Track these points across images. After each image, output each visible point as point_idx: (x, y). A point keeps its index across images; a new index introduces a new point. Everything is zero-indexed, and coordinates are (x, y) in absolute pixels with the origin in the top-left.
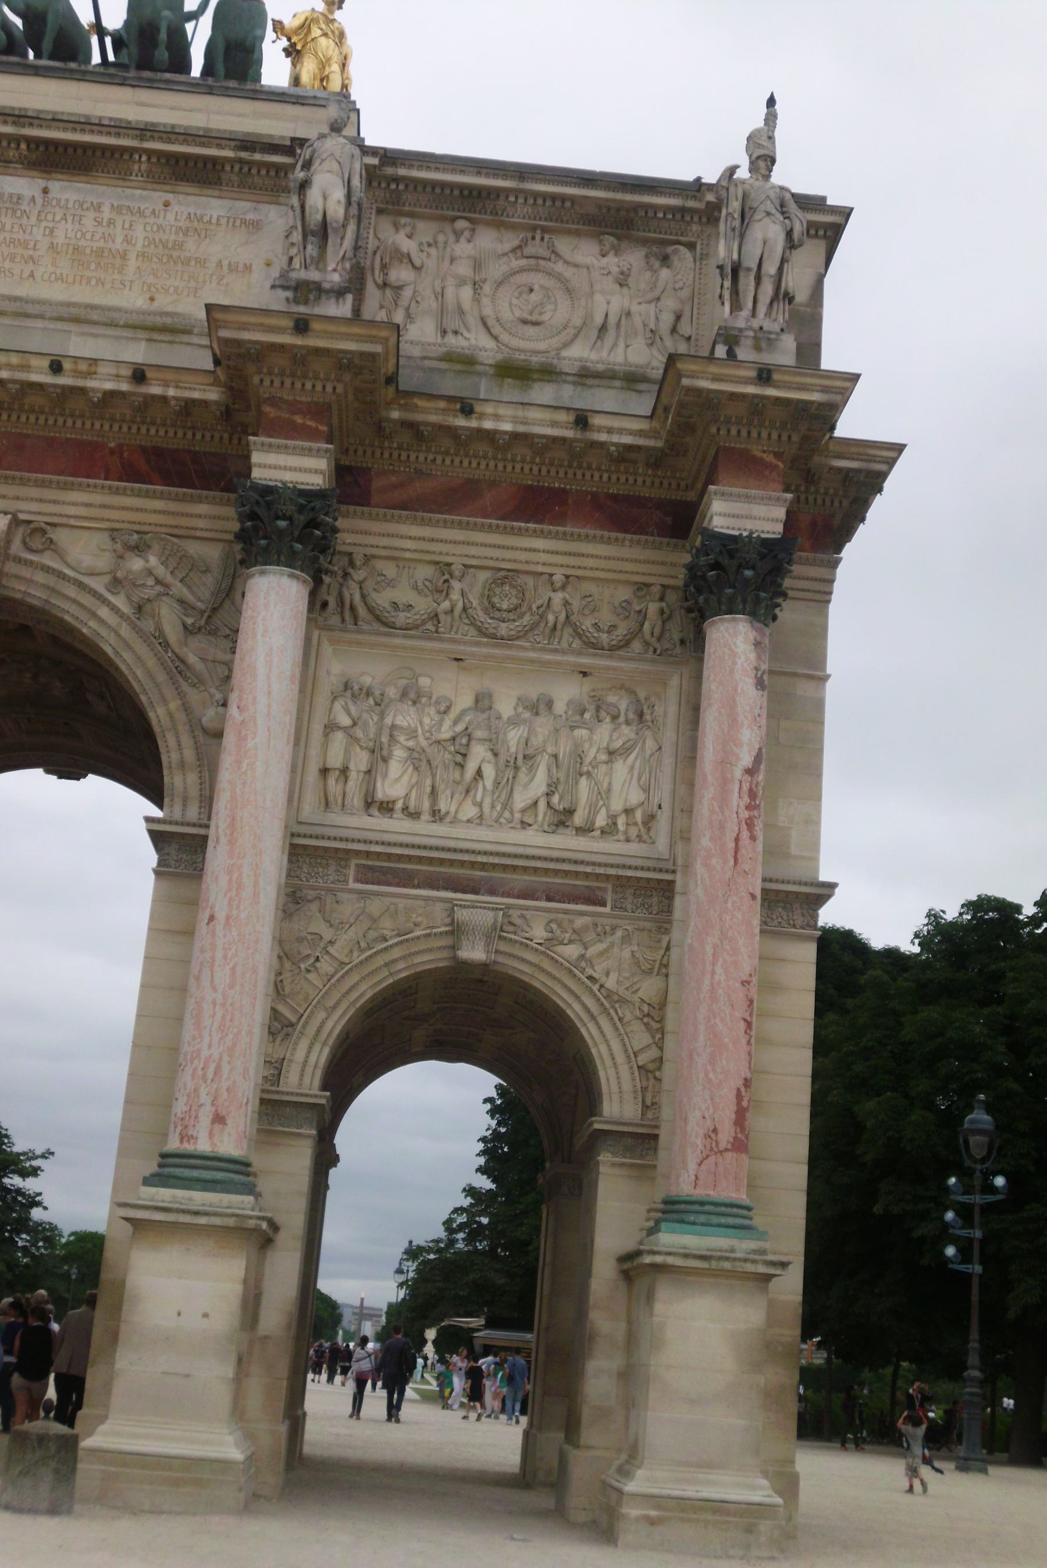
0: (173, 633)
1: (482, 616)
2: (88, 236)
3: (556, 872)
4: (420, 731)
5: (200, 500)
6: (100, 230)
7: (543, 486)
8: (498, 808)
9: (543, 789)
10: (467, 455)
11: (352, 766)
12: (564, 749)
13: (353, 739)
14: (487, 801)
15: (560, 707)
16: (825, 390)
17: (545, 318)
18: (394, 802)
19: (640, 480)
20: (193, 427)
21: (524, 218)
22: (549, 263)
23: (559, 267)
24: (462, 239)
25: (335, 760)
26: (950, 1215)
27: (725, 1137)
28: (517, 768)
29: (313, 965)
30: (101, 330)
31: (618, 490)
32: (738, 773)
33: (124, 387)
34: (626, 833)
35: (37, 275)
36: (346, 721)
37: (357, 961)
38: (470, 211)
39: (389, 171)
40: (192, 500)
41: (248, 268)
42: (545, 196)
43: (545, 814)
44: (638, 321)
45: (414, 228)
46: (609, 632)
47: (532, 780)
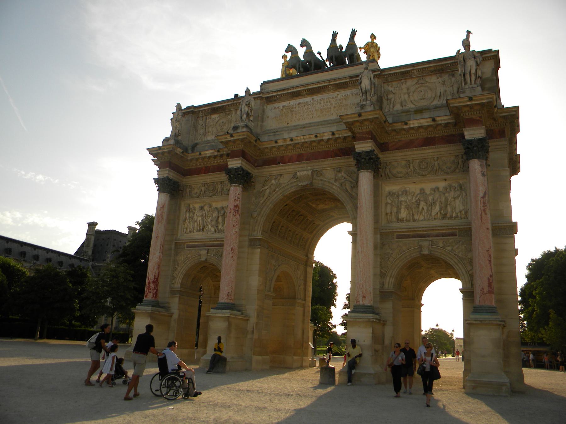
0: (349, 189)
2: (323, 106)
3: (443, 229)
4: (408, 201)
6: (325, 104)
7: (429, 137)
8: (429, 216)
9: (439, 209)
10: (409, 134)
11: (393, 212)
12: (443, 199)
14: (426, 215)
15: (441, 189)
16: (487, 99)
17: (426, 97)
18: (403, 218)
19: (452, 130)
20: (347, 142)
21: (417, 75)
22: (425, 84)
23: (428, 84)
24: (404, 84)
25: (388, 210)
27: (486, 290)
28: (432, 206)
29: (388, 259)
31: (448, 134)
32: (479, 198)
33: (331, 137)
34: (461, 217)
36: (390, 202)
37: (398, 257)
38: (404, 77)
39: (383, 73)
42: (420, 69)
43: (440, 215)
45: (392, 84)
46: (450, 169)
47: (436, 207)
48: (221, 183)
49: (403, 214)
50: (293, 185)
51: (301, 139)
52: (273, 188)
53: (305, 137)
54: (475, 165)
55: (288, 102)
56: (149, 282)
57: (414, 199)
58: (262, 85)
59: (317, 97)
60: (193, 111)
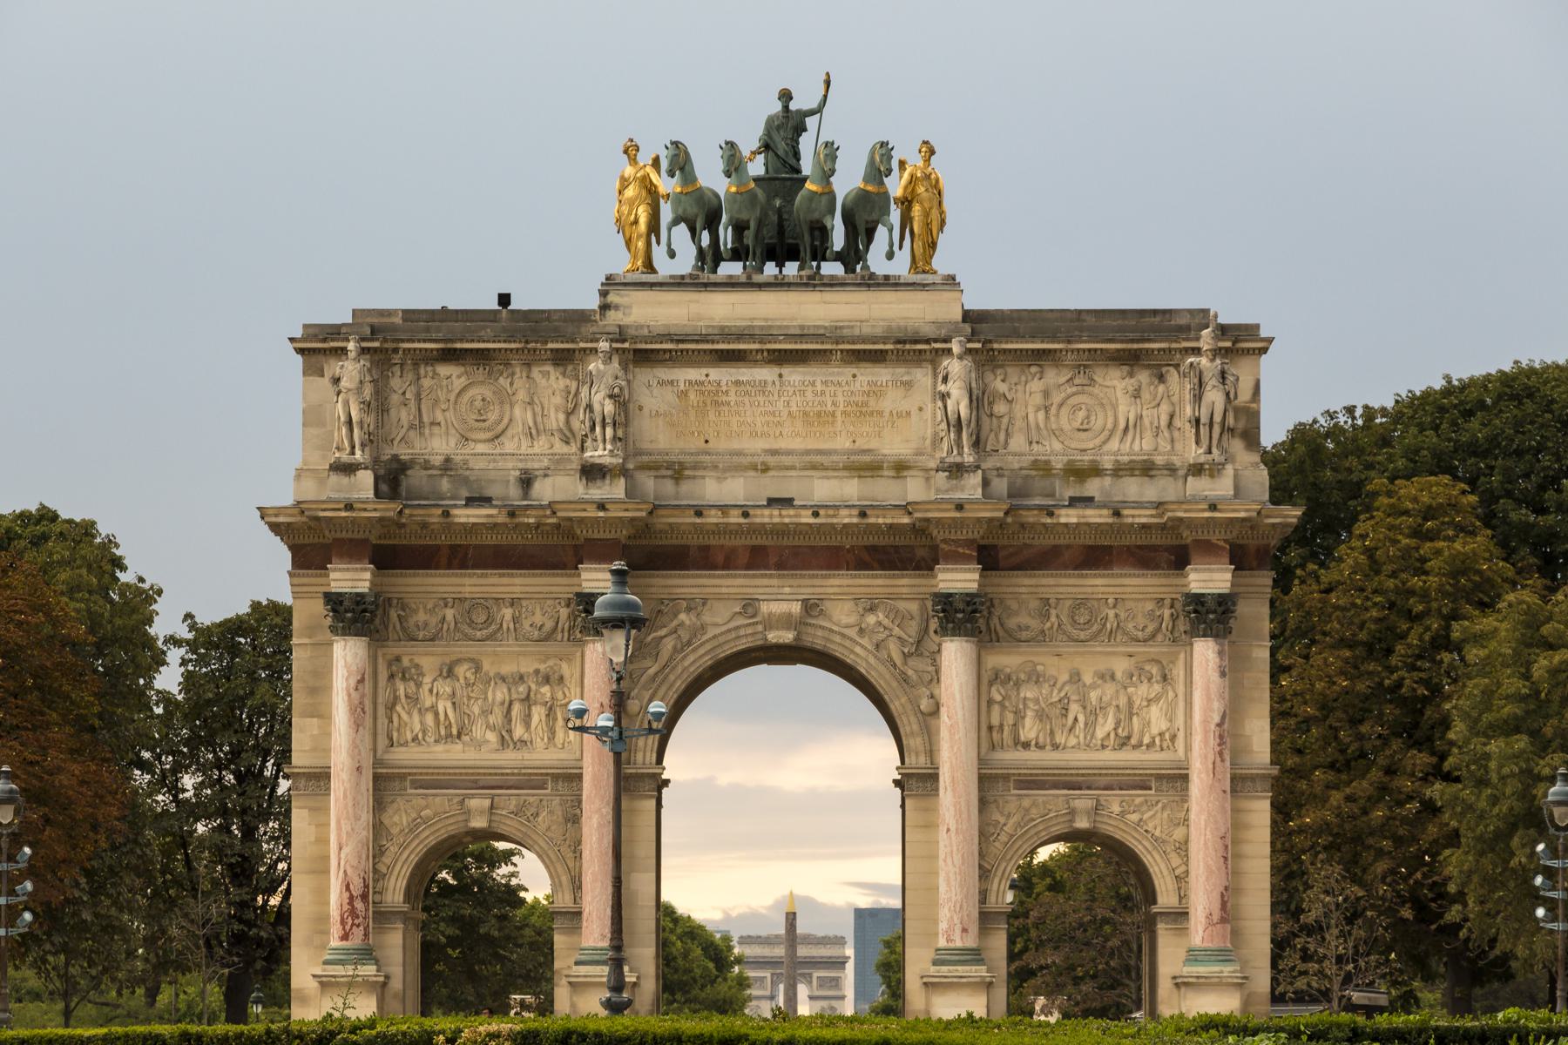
1: (1069, 628)
5: (903, 577)
6: (818, 399)
9: (1113, 726)
12: (1123, 701)
13: (1003, 707)
15: (1119, 675)
23: (1096, 390)
25: (995, 721)
26: (1539, 880)
27: (1216, 918)
30: (831, 473)
33: (855, 520)
35: (784, 433)
36: (998, 698)
40: (899, 577)
41: (909, 414)
42: (1084, 350)
44: (1146, 421)
45: (1006, 375)
48: (513, 603)
49: (1029, 730)
50: (742, 632)
51: (771, 516)
52: (685, 636)
53: (784, 512)
54: (1205, 652)
55: (704, 371)
56: (351, 898)
57: (1056, 691)
58: (604, 294)
59: (795, 375)
60: (375, 350)
